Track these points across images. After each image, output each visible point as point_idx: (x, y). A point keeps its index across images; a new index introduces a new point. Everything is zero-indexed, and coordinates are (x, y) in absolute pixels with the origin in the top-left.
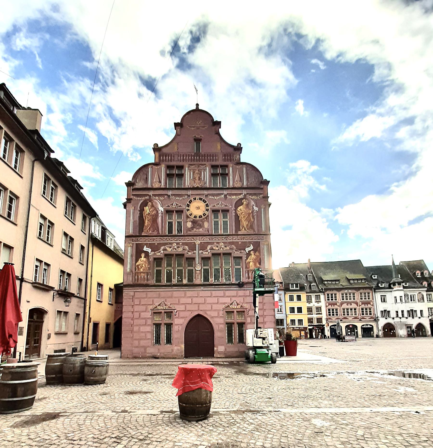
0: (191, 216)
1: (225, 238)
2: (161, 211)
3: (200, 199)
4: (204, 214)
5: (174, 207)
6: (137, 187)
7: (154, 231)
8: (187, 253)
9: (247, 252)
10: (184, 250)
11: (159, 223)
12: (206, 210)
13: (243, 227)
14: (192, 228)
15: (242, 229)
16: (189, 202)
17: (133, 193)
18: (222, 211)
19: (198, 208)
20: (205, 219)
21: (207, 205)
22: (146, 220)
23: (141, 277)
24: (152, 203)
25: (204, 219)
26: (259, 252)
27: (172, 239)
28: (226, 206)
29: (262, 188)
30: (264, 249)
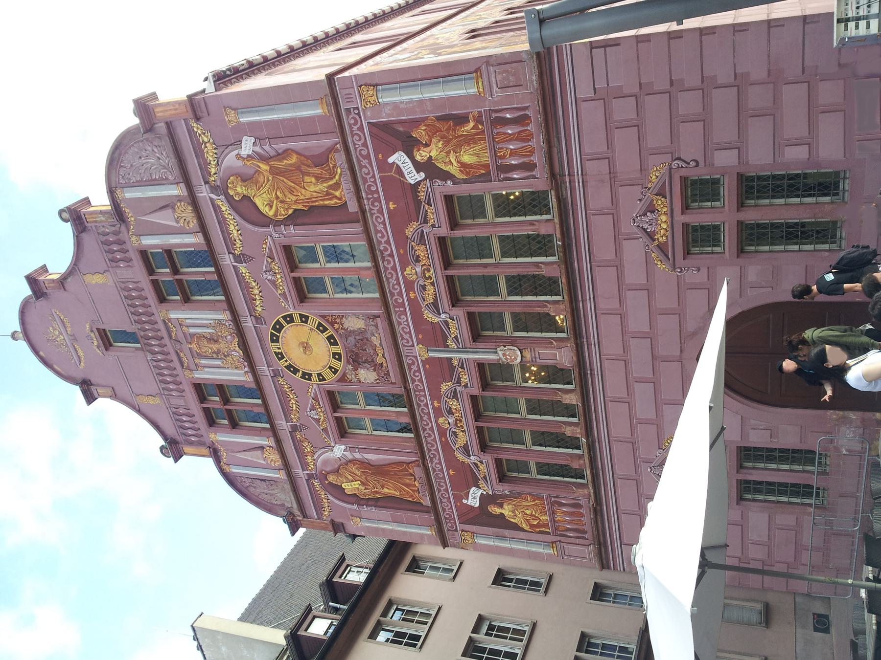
1: (383, 259)
3: (275, 339)
4: (321, 328)
5: (322, 414)
6: (295, 506)
7: (412, 475)
8: (466, 386)
9: (423, 175)
10: (455, 396)
12: (306, 322)
13: (328, 195)
14: (377, 367)
17: (316, 517)
19: (306, 347)
21: (289, 319)
22: (380, 489)
23: (569, 522)
25: (337, 331)
26: (416, 123)
27: (427, 428)
29: (169, 125)
30: (395, 105)
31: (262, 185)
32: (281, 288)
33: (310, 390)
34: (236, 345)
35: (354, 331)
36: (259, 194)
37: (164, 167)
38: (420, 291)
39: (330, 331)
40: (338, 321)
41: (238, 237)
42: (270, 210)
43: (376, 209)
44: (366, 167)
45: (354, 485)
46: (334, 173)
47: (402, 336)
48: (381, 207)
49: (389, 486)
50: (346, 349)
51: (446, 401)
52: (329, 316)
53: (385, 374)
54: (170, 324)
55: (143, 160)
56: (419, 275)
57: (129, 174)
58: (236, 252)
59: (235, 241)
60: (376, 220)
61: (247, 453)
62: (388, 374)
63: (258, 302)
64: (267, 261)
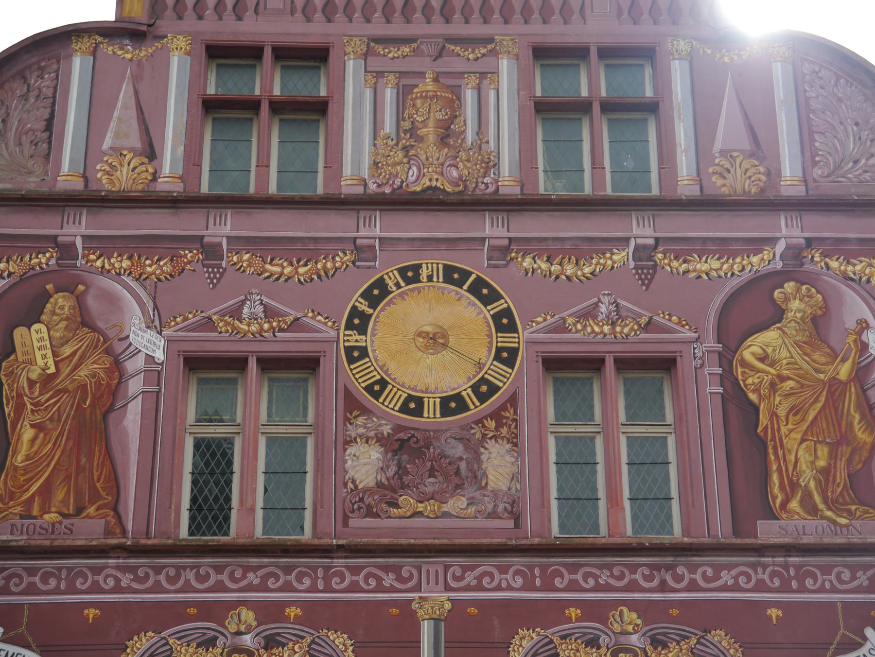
0: (377, 395)
1: (653, 567)
2: (150, 359)
7: (79, 510)
11: (125, 450)
12: (497, 357)
13: (791, 486)
15: (784, 505)
16: (367, 295)
18: (617, 361)
20: (492, 424)
24: (80, 300)
25: (480, 422)
27: (224, 577)
28: (649, 326)
31: (807, 354)
32: (579, 327)
33: (319, 318)
34: (434, 183)
35: (479, 461)
36: (787, 342)
37: (838, 167)
38: (585, 634)
39: (476, 408)
40: (504, 431)
41: (694, 270)
42: (753, 354)
43: (766, 577)
44: (854, 578)
45: (44, 357)
46: (839, 509)
47: (473, 568)
48: (770, 590)
49: (43, 445)
50: (434, 431)
51: (303, 638)
52: (515, 413)
53: (369, 507)
54: (483, 51)
55: (852, 129)
56: (623, 639)
57: (822, 88)
58: (660, 256)
59: (685, 262)
60: (742, 573)
61: (133, 112)
62: (370, 513)
63: (544, 266)
64: (640, 316)
